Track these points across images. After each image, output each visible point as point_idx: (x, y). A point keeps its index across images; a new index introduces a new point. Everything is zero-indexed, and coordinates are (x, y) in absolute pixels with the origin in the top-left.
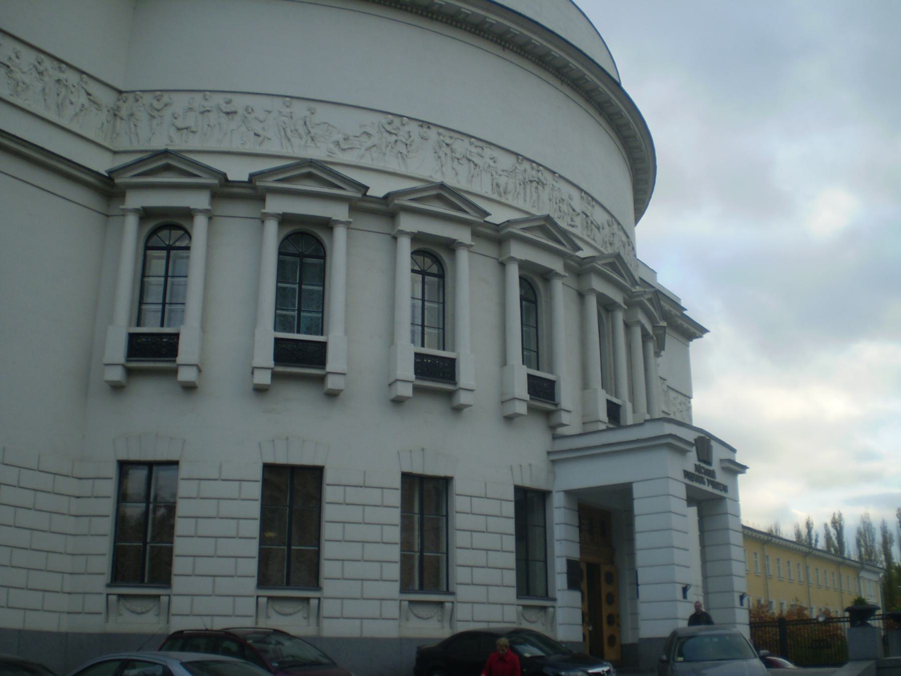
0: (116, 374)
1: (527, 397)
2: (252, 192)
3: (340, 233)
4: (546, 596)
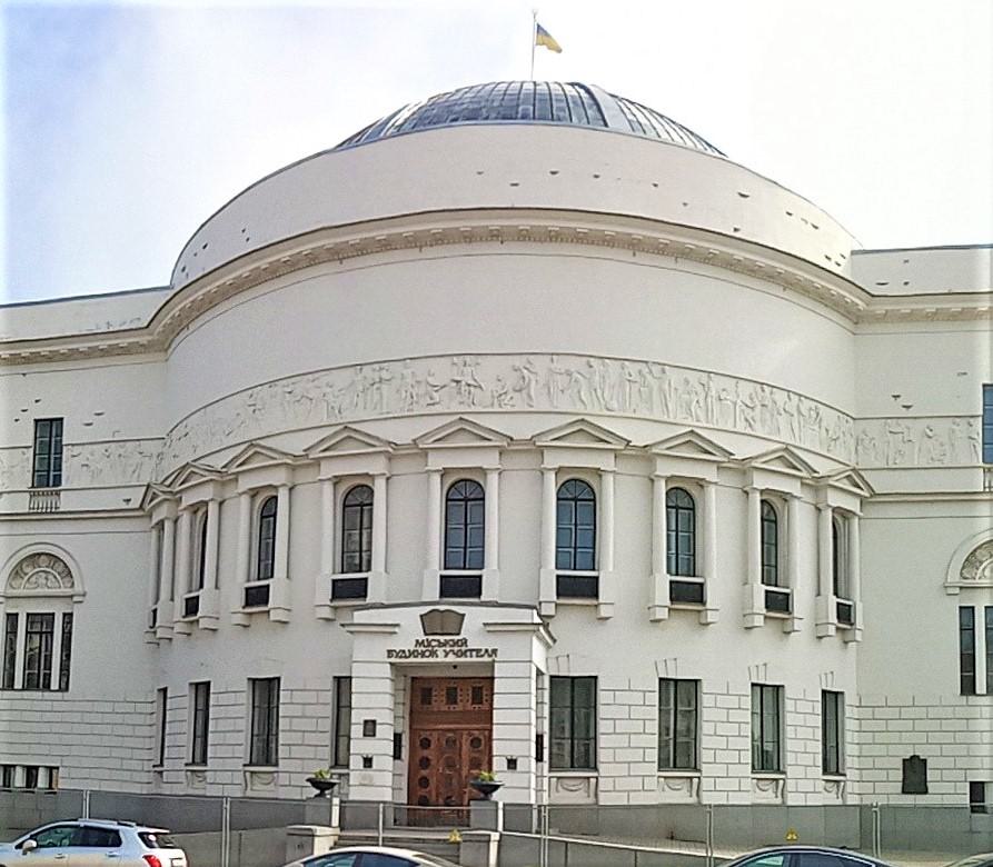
0: (327, 613)
1: (668, 603)
2: (417, 451)
3: (493, 479)
4: (696, 769)
